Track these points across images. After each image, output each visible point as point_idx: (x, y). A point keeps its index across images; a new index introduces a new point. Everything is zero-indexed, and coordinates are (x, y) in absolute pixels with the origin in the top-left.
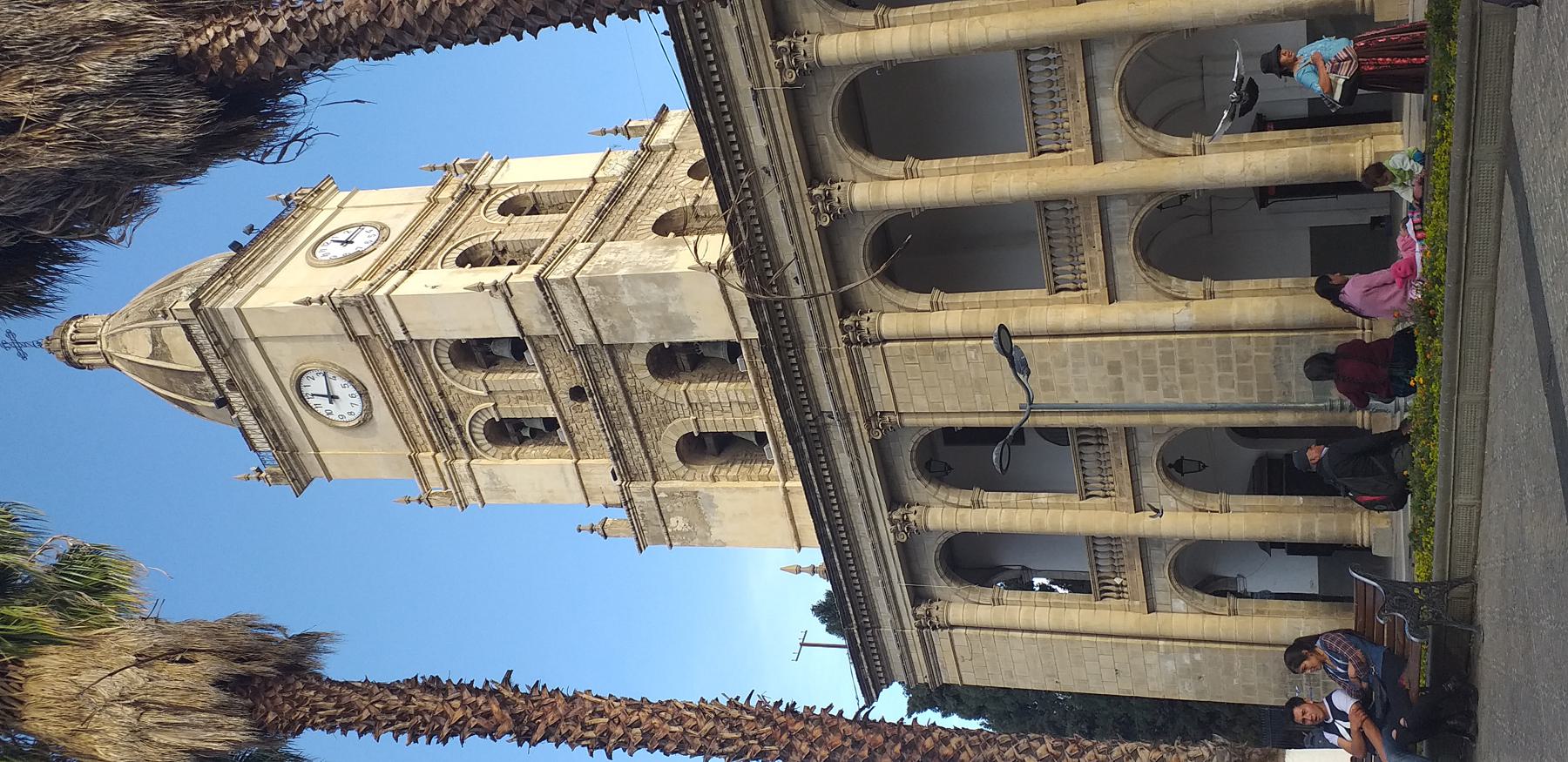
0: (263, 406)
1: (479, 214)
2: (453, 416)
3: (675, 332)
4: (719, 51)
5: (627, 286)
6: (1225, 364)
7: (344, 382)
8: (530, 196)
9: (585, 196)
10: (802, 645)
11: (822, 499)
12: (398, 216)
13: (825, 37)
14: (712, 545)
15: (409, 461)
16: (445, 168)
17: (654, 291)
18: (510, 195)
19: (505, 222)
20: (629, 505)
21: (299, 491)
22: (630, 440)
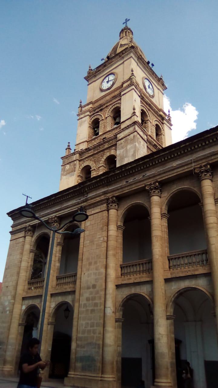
0: (106, 67)
2: (101, 110)
3: (119, 161)
4: (206, 147)
5: (133, 146)
6: (92, 326)
7: (112, 84)
8: (161, 133)
10: (27, 197)
12: (156, 101)
14: (61, 177)
15: (90, 101)
16: (169, 115)
18: (161, 128)
19: (154, 125)
21: (85, 78)
22: (91, 153)
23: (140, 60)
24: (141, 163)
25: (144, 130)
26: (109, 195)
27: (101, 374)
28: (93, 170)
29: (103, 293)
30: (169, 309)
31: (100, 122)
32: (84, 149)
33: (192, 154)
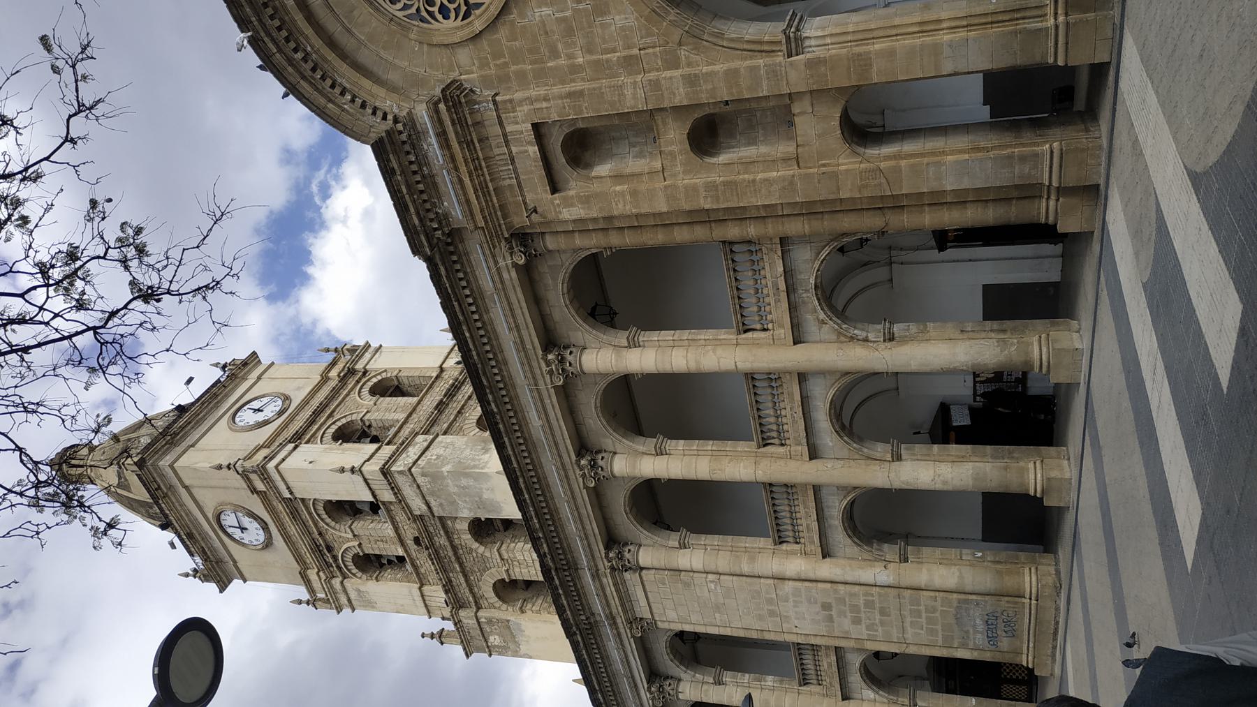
1: (355, 393)
2: (329, 549)
3: (489, 511)
4: (500, 358)
5: (451, 479)
7: (250, 520)
9: (433, 382)
11: (595, 674)
12: (299, 388)
13: (587, 351)
14: (521, 657)
15: (299, 576)
17: (472, 483)
19: (372, 403)
20: (458, 625)
23: (178, 437)
24: (527, 496)
25: (402, 444)
26: (603, 565)
27: (1024, 600)
28: (509, 575)
29: (841, 587)
30: (878, 455)
31: (367, 552)
32: (444, 596)
33: (514, 387)
